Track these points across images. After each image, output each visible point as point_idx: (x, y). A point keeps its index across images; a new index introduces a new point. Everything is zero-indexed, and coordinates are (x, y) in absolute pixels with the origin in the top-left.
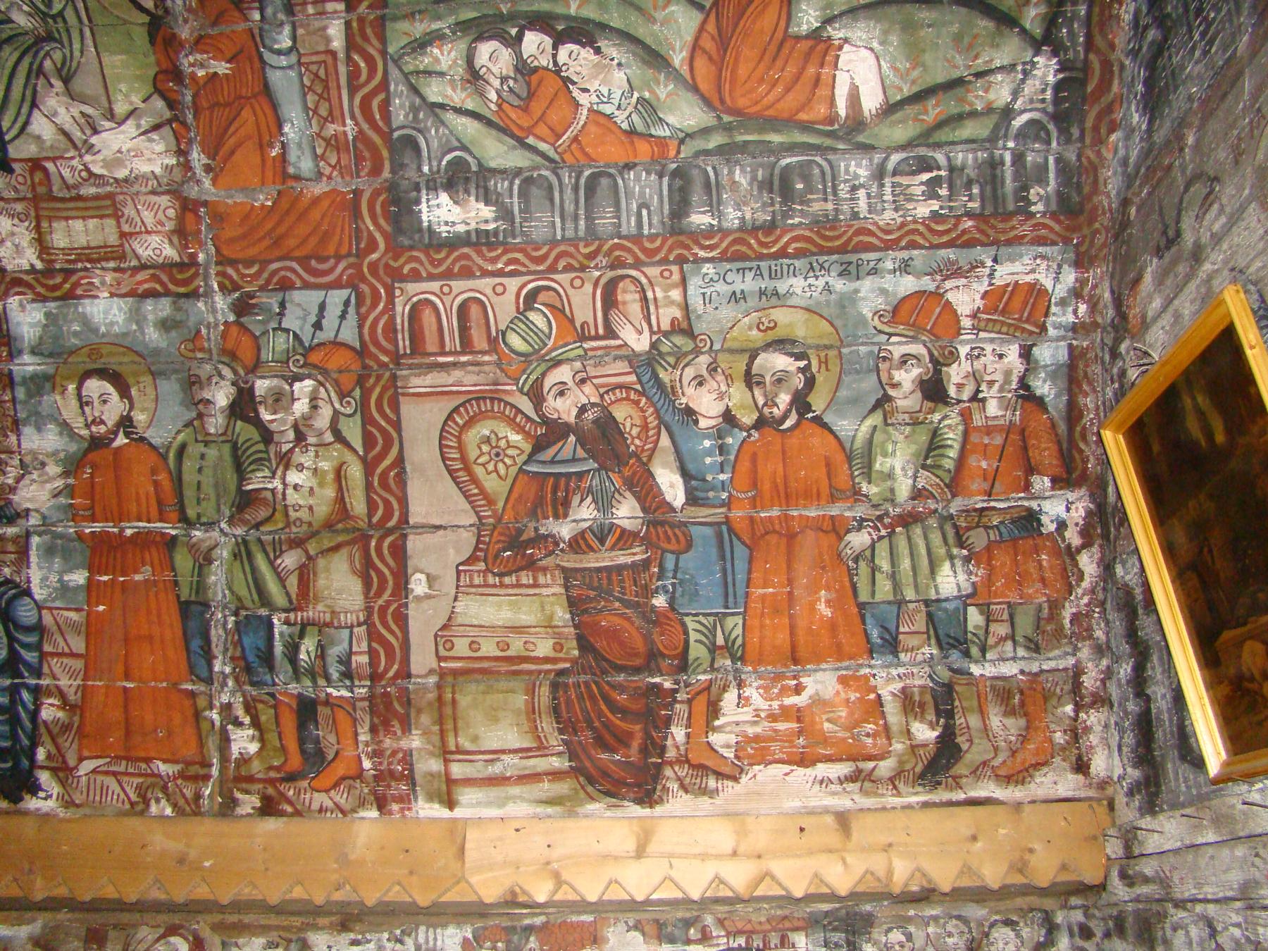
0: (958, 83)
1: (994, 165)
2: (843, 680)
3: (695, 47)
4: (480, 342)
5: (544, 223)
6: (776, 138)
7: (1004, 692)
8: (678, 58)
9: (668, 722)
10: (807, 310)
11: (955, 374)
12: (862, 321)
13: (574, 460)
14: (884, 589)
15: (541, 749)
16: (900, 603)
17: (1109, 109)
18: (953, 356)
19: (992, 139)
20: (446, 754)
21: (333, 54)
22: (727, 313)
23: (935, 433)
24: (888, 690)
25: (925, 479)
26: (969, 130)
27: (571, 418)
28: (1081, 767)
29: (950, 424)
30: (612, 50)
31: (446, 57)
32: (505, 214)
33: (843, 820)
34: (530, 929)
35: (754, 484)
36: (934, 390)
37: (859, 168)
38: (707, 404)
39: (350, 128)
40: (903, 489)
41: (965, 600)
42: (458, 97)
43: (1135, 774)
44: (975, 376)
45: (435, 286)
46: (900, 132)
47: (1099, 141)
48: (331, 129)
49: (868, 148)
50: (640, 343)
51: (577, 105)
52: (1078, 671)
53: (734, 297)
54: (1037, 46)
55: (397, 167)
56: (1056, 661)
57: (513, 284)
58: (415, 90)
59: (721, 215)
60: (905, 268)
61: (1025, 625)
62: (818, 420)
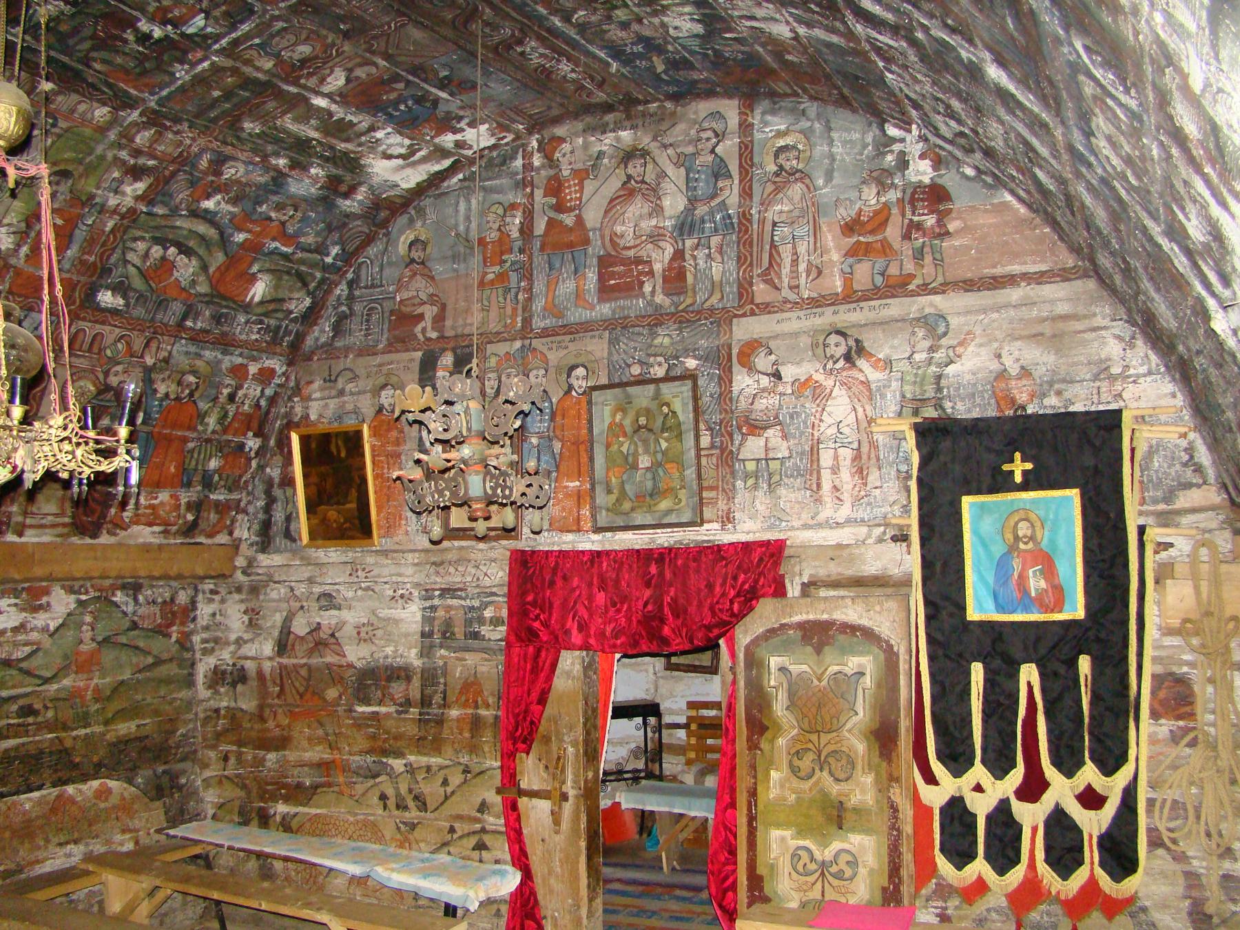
0: (283, 300)
1: (279, 327)
2: (171, 496)
3: (219, 268)
4: (95, 350)
5: (139, 312)
6: (224, 303)
7: (217, 504)
8: (211, 270)
9: (111, 506)
10: (207, 363)
11: (240, 393)
12: (221, 370)
13: (109, 401)
14: (194, 463)
15: (63, 514)
16: (196, 470)
17: (317, 319)
18: (241, 387)
19: (283, 320)
20: (25, 514)
21: (104, 232)
22: (182, 358)
23: (226, 413)
24: (184, 501)
25: (218, 428)
26: (280, 315)
27: (115, 385)
28: (231, 534)
29: (232, 409)
30: (194, 262)
31: (141, 246)
32: (127, 305)
33: (160, 547)
34: (23, 589)
35: (166, 421)
36: (232, 398)
37: (242, 319)
38: (162, 389)
39: (92, 259)
40: (210, 428)
41: (216, 471)
42: (137, 262)
43: (255, 538)
44: (246, 396)
45: (89, 324)
46: (259, 310)
47: (311, 326)
48: (86, 257)
49: (247, 313)
50: (149, 361)
51: (172, 275)
52: (240, 500)
53: (187, 353)
54: (309, 294)
55: (101, 277)
56: (235, 496)
57: (117, 330)
58: (124, 253)
59: (195, 323)
60: (241, 355)
61: (230, 481)
62: (194, 402)
